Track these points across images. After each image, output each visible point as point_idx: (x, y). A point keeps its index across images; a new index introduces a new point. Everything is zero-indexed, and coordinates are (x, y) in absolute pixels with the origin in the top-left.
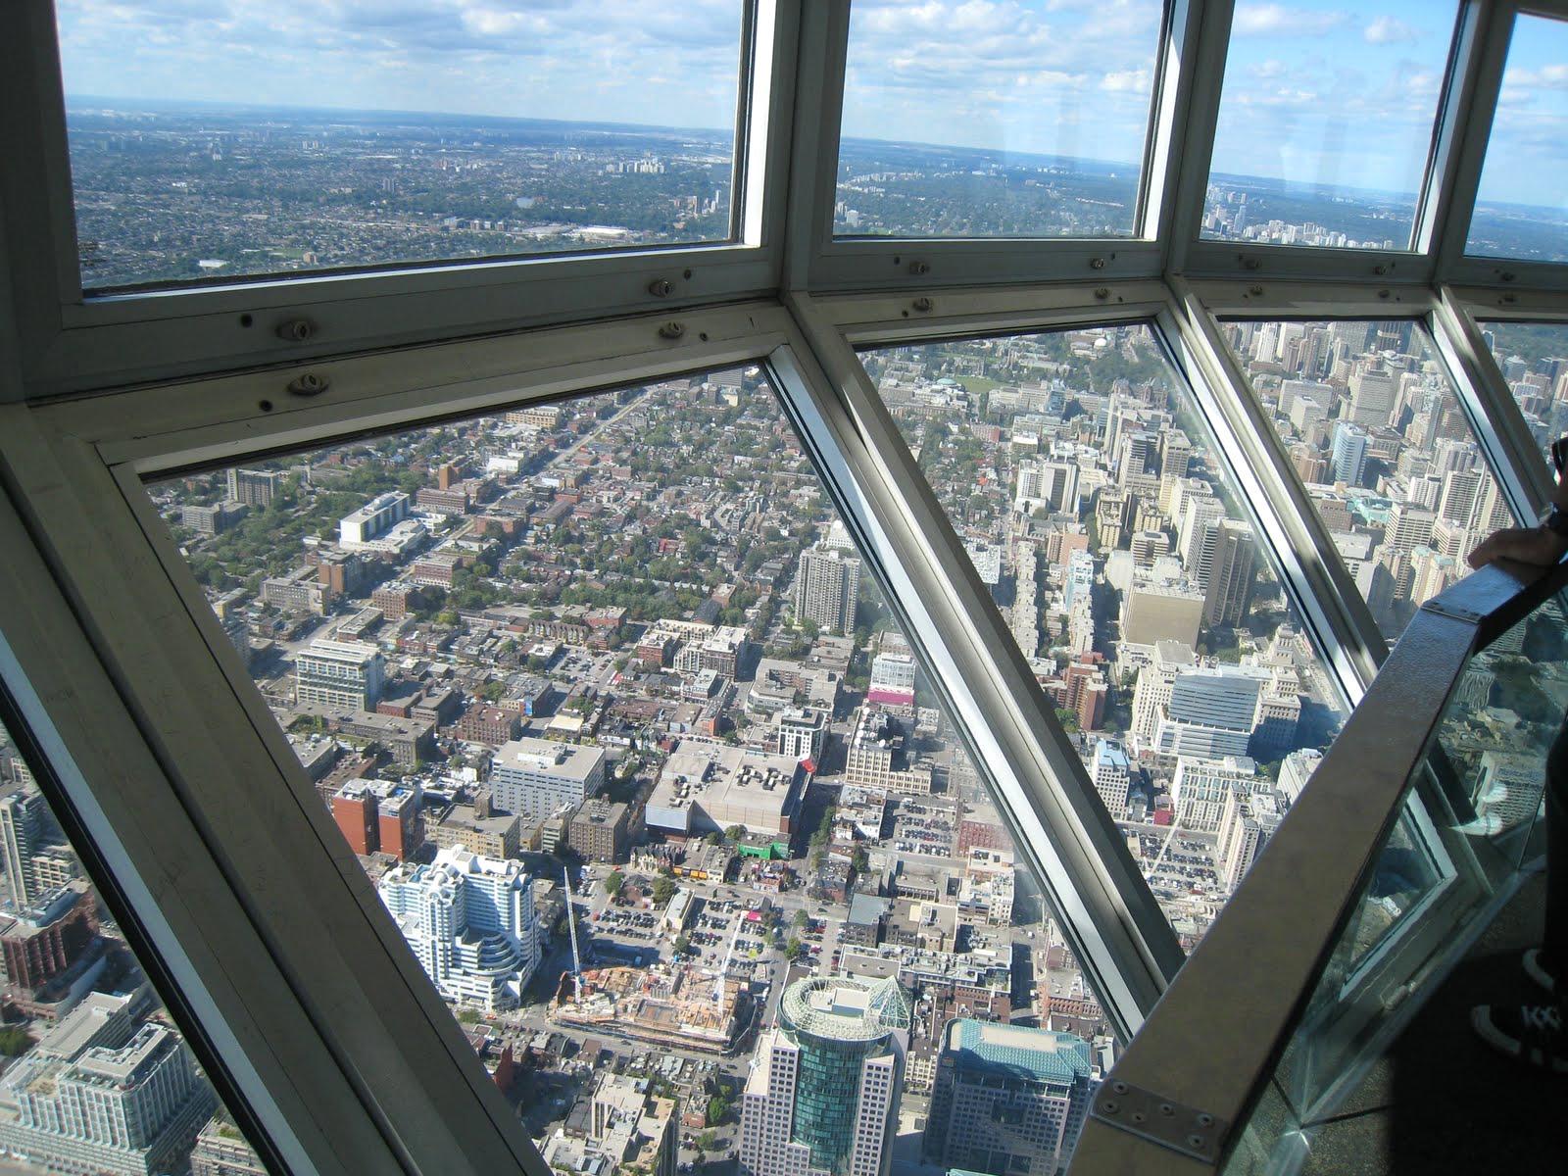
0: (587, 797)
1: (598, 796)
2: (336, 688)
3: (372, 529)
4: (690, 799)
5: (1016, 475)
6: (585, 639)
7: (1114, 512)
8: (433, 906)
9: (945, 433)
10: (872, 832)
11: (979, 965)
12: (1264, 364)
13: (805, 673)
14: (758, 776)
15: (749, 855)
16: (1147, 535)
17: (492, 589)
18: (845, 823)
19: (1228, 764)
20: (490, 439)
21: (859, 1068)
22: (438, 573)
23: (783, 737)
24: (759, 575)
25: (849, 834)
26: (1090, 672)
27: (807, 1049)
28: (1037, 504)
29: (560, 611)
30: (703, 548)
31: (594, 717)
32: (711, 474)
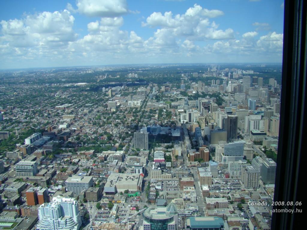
0: (89, 187)
1: (92, 186)
2: (26, 172)
3: (33, 141)
4: (115, 185)
5: (180, 117)
6: (86, 157)
7: (203, 120)
8: (52, 210)
9: (163, 111)
10: (160, 188)
11: (191, 210)
12: (230, 92)
13: (138, 158)
14: (130, 178)
15: (131, 196)
16: (211, 123)
17: (62, 150)
18: (153, 186)
19: (240, 162)
20: (59, 122)
21: (167, 227)
22: (49, 148)
23: (135, 170)
24: (125, 141)
25: (154, 189)
26: (204, 149)
27: (152, 223)
28: (185, 121)
29: (79, 153)
30: (110, 138)
31: (89, 172)
32: (111, 124)
